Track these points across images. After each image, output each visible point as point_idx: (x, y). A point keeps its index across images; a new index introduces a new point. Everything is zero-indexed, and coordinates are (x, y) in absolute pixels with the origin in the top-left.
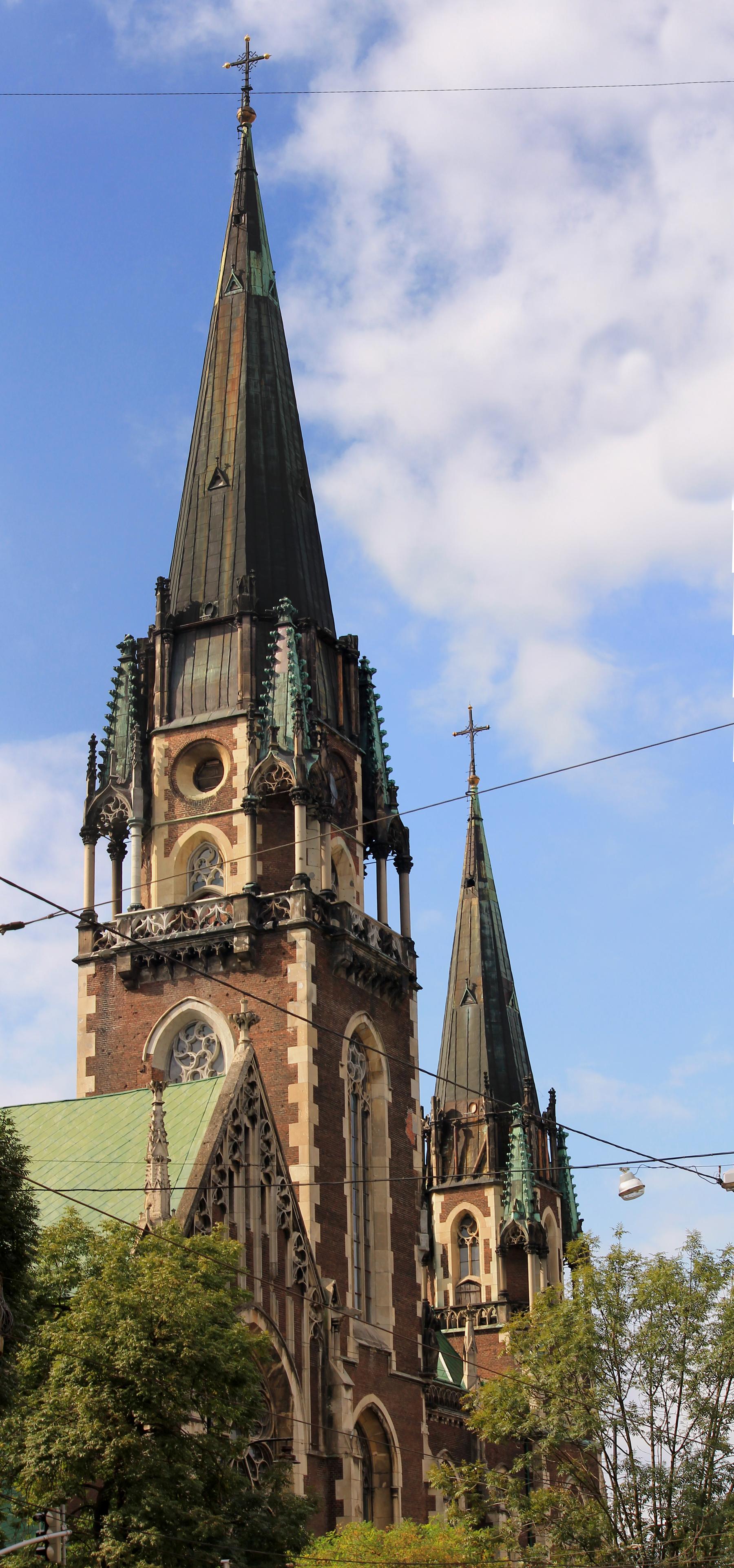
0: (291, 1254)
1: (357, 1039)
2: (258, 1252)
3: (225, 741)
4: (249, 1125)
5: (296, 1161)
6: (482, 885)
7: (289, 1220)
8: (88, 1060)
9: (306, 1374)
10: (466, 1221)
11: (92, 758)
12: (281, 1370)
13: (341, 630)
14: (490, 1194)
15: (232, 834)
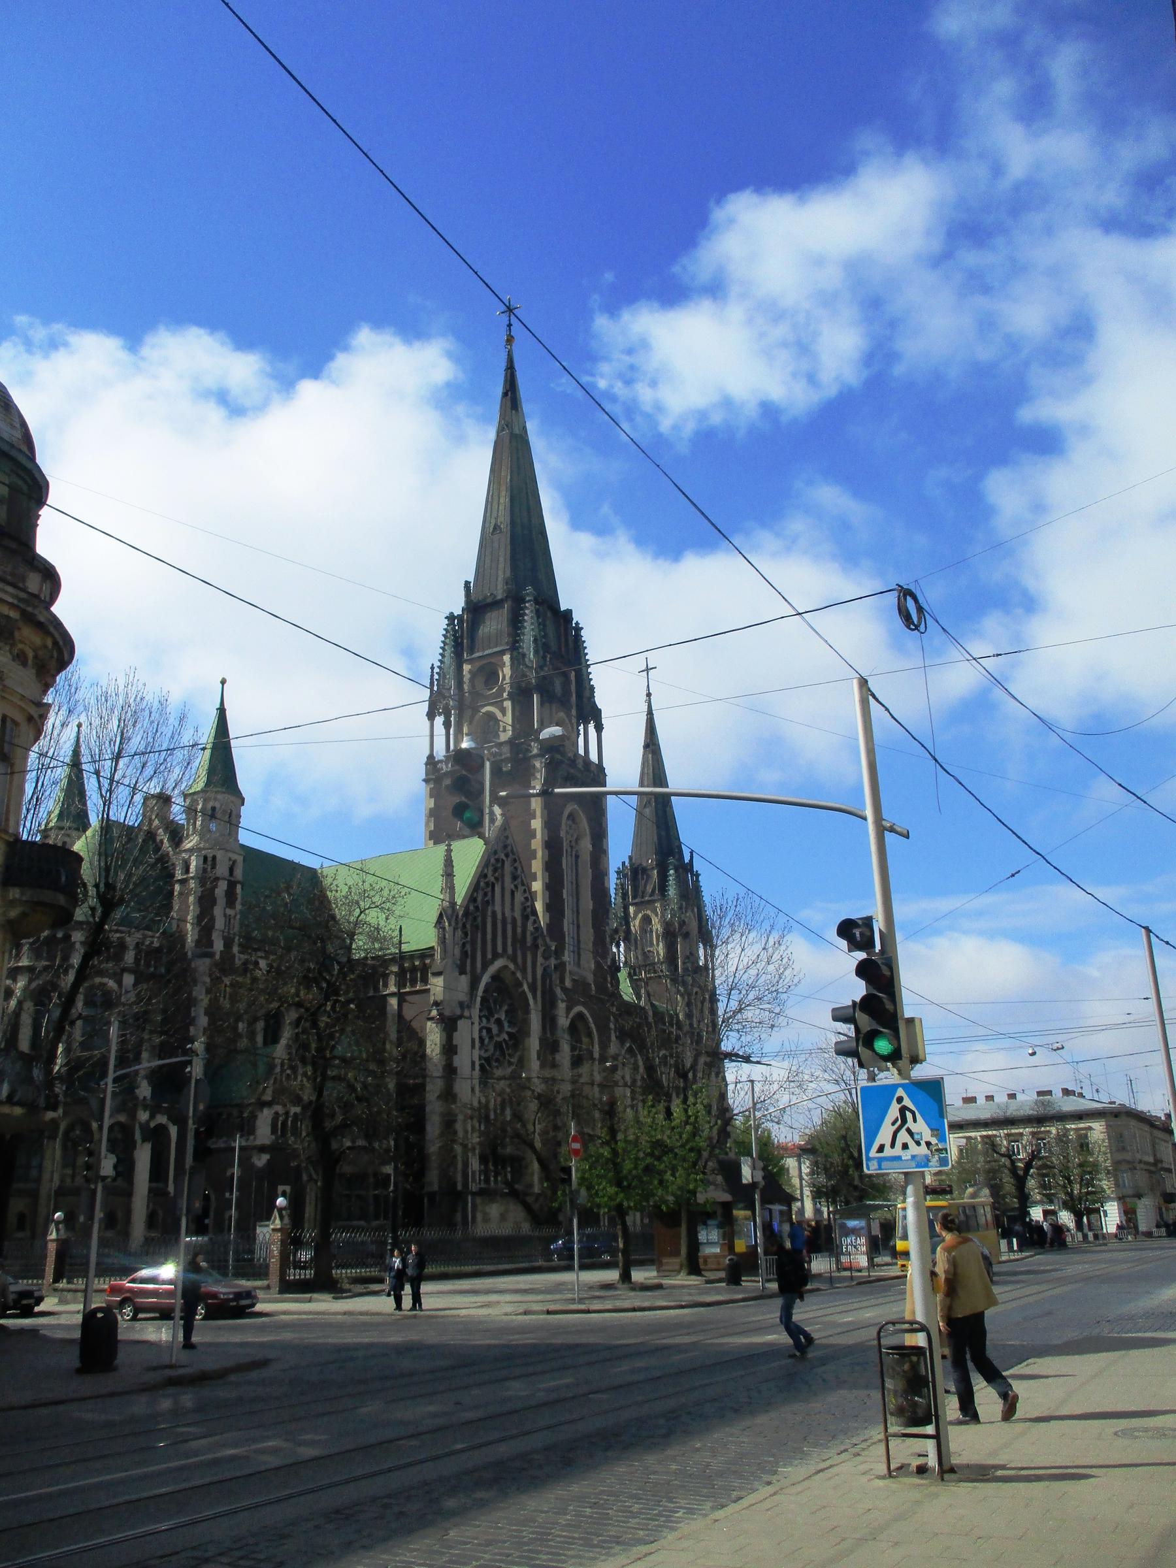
0: (530, 927)
1: (571, 817)
2: (509, 928)
3: (499, 663)
4: (504, 858)
5: (535, 880)
6: (654, 747)
7: (529, 910)
8: (430, 832)
9: (539, 994)
10: (647, 920)
11: (432, 676)
12: (524, 992)
13: (563, 607)
14: (658, 905)
15: (504, 713)
